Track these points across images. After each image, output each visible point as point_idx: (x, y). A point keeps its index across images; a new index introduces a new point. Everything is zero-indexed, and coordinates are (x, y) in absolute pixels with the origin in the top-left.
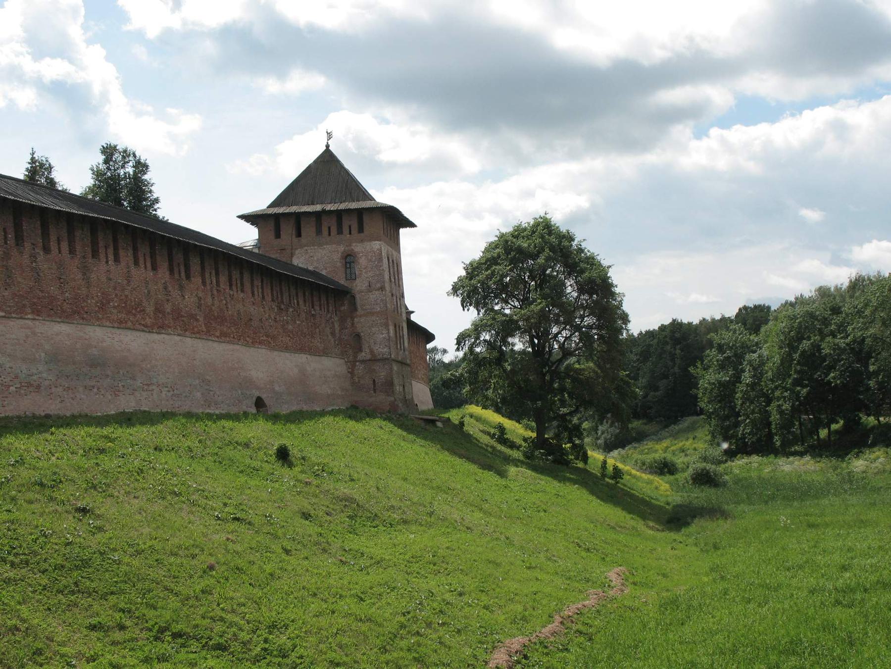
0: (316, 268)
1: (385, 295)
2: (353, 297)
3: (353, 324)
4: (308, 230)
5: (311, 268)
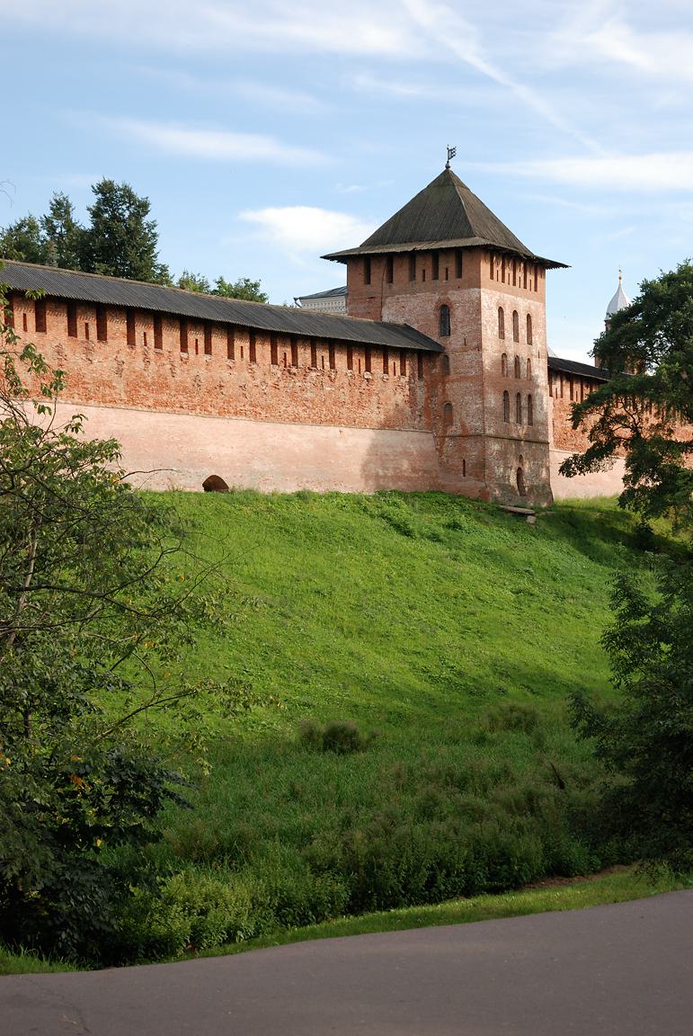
0: (407, 320)
2: (447, 357)
3: (444, 391)
4: (401, 273)
5: (401, 321)
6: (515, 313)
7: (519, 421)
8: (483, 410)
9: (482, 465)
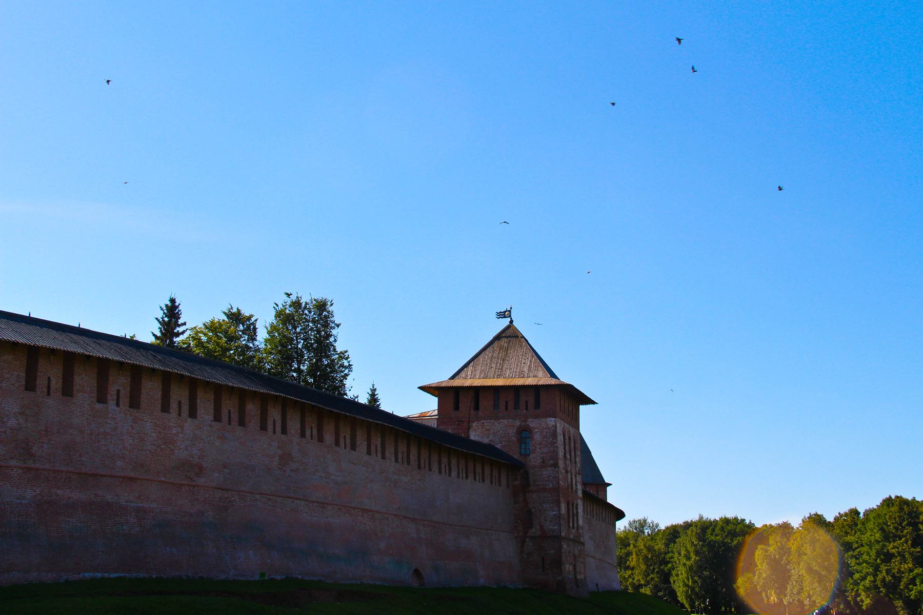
1: (557, 472)
2: (527, 473)
4: (486, 403)
5: (486, 441)
6: (569, 438)
8: (559, 517)
9: (558, 563)
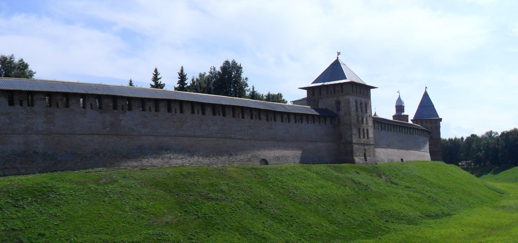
5: (324, 107)
6: (361, 103)
7: (364, 137)
